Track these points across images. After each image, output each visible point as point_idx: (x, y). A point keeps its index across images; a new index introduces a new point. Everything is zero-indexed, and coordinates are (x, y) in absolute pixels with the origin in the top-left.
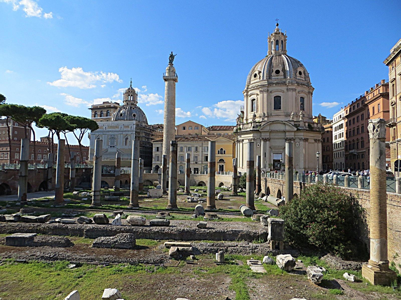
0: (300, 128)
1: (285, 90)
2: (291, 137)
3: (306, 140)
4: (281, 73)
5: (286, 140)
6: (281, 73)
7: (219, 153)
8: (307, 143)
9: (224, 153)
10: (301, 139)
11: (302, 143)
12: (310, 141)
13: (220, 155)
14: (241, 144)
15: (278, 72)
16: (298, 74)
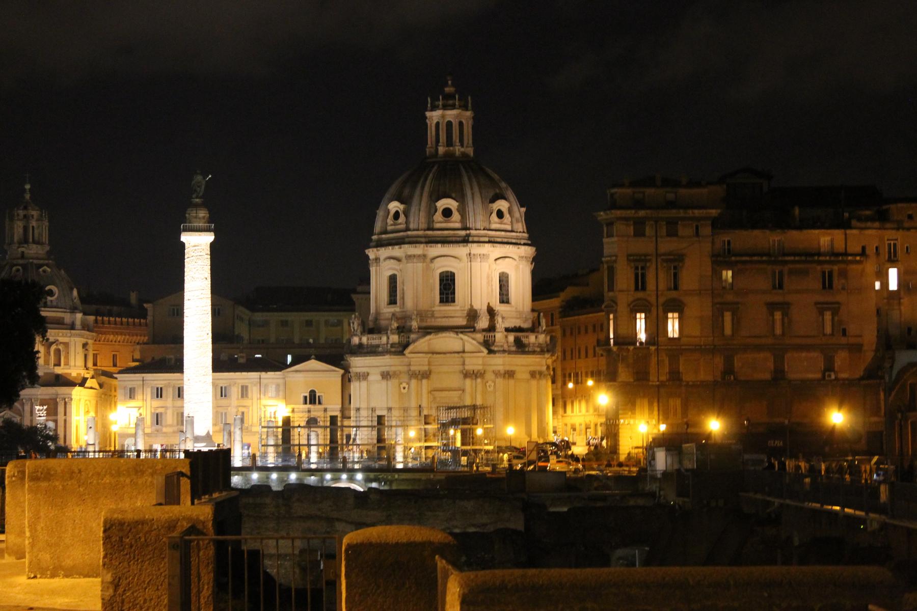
0: (496, 349)
1: (465, 258)
2: (476, 368)
3: (510, 374)
4: (456, 216)
5: (466, 375)
6: (456, 216)
7: (305, 403)
8: (512, 382)
9: (320, 403)
10: (497, 374)
11: (500, 381)
12: (518, 375)
13: (308, 406)
14: (364, 384)
15: (447, 213)
16: (494, 215)
